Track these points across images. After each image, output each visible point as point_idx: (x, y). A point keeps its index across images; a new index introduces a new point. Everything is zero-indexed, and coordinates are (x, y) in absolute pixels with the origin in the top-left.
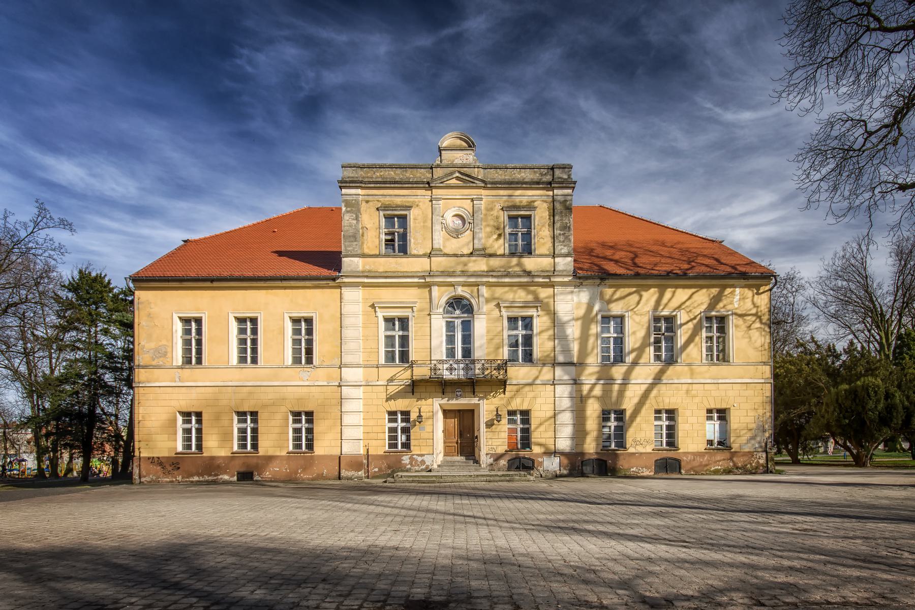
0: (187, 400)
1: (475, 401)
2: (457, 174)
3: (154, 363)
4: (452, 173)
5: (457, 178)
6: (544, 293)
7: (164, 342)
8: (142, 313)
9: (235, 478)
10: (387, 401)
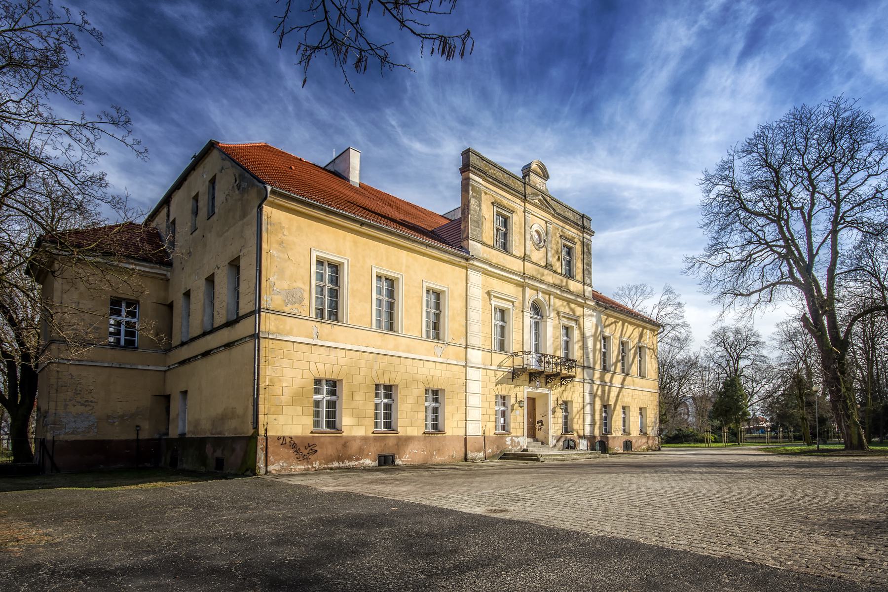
0: (324, 365)
1: (545, 391)
2: (540, 197)
3: (287, 309)
4: (537, 195)
5: (540, 200)
6: (579, 311)
7: (299, 284)
8: (273, 239)
9: (375, 464)
10: (497, 384)
